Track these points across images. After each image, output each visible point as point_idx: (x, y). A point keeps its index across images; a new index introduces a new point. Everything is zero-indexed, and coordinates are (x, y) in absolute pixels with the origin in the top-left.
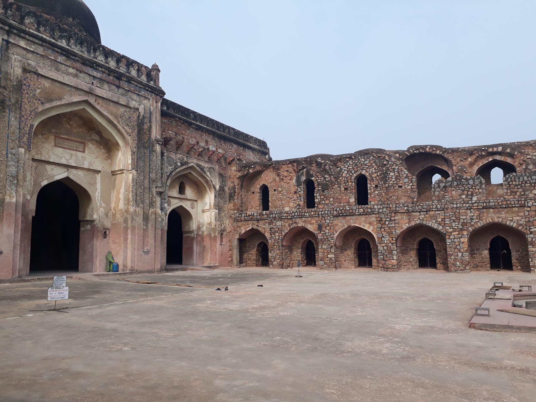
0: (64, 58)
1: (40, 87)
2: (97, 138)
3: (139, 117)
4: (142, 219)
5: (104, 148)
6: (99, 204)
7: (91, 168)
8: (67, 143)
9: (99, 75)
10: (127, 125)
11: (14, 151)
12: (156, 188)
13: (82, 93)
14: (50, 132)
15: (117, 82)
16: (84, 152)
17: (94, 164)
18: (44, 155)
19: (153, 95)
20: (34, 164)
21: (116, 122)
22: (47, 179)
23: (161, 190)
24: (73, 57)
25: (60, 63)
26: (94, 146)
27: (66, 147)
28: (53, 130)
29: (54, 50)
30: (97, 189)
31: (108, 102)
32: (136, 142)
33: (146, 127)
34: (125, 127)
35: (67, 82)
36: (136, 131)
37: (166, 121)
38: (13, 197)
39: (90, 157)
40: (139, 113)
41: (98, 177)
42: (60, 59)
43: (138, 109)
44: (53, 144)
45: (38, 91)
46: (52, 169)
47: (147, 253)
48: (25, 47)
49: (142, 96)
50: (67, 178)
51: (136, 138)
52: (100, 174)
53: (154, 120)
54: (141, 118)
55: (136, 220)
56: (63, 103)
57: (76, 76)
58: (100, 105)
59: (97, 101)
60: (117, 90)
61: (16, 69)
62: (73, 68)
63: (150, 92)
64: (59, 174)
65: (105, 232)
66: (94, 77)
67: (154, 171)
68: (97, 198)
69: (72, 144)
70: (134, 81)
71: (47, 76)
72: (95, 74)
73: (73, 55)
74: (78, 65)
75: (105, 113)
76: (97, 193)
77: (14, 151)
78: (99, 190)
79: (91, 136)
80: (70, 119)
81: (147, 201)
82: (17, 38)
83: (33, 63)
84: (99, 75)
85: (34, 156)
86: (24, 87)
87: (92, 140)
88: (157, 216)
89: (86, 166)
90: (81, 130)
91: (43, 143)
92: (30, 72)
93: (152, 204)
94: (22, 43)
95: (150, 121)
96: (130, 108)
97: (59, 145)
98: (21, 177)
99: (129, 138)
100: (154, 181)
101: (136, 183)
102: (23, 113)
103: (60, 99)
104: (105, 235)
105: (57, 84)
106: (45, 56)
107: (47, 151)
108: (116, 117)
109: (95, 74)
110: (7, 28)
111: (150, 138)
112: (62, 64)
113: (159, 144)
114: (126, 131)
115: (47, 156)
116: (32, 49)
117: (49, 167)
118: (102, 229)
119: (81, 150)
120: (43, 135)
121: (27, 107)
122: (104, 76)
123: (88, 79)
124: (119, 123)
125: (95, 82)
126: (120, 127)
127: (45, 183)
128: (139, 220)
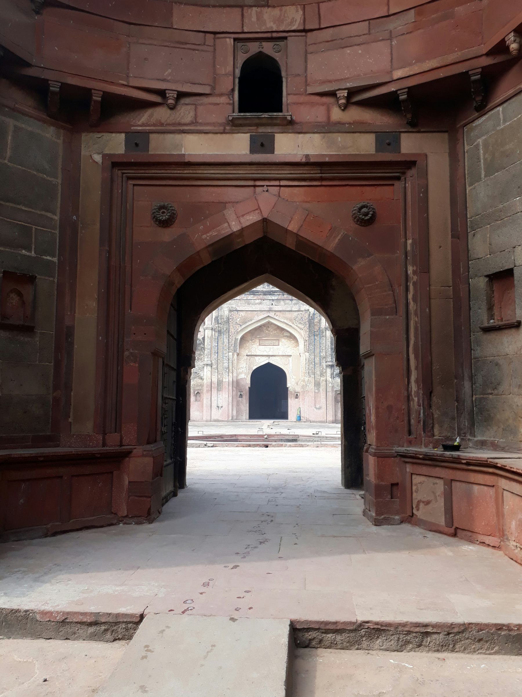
0: (252, 296)
2: (288, 334)
5: (293, 340)
8: (267, 342)
9: (276, 298)
10: (300, 323)
11: (226, 355)
13: (265, 312)
14: (256, 338)
20: (248, 358)
21: (291, 324)
23: (330, 364)
26: (286, 340)
31: (284, 312)
32: (307, 333)
33: (316, 320)
36: (308, 326)
41: (290, 359)
43: (308, 310)
44: (258, 344)
45: (238, 320)
47: (320, 408)
56: (253, 321)
57: (260, 303)
60: (291, 302)
61: (225, 312)
62: (258, 299)
64: (263, 361)
65: (297, 395)
66: (273, 300)
67: (324, 351)
72: (273, 298)
74: (261, 296)
75: (282, 320)
77: (226, 355)
81: (318, 373)
83: (234, 306)
86: (230, 320)
88: (328, 382)
92: (233, 311)
98: (231, 368)
102: (230, 334)
104: (297, 397)
108: (291, 320)
109: (273, 298)
111: (320, 328)
114: (299, 327)
118: (293, 393)
120: (252, 340)
121: (233, 330)
122: (280, 297)
123: (268, 302)
125: (273, 303)
128: (311, 386)
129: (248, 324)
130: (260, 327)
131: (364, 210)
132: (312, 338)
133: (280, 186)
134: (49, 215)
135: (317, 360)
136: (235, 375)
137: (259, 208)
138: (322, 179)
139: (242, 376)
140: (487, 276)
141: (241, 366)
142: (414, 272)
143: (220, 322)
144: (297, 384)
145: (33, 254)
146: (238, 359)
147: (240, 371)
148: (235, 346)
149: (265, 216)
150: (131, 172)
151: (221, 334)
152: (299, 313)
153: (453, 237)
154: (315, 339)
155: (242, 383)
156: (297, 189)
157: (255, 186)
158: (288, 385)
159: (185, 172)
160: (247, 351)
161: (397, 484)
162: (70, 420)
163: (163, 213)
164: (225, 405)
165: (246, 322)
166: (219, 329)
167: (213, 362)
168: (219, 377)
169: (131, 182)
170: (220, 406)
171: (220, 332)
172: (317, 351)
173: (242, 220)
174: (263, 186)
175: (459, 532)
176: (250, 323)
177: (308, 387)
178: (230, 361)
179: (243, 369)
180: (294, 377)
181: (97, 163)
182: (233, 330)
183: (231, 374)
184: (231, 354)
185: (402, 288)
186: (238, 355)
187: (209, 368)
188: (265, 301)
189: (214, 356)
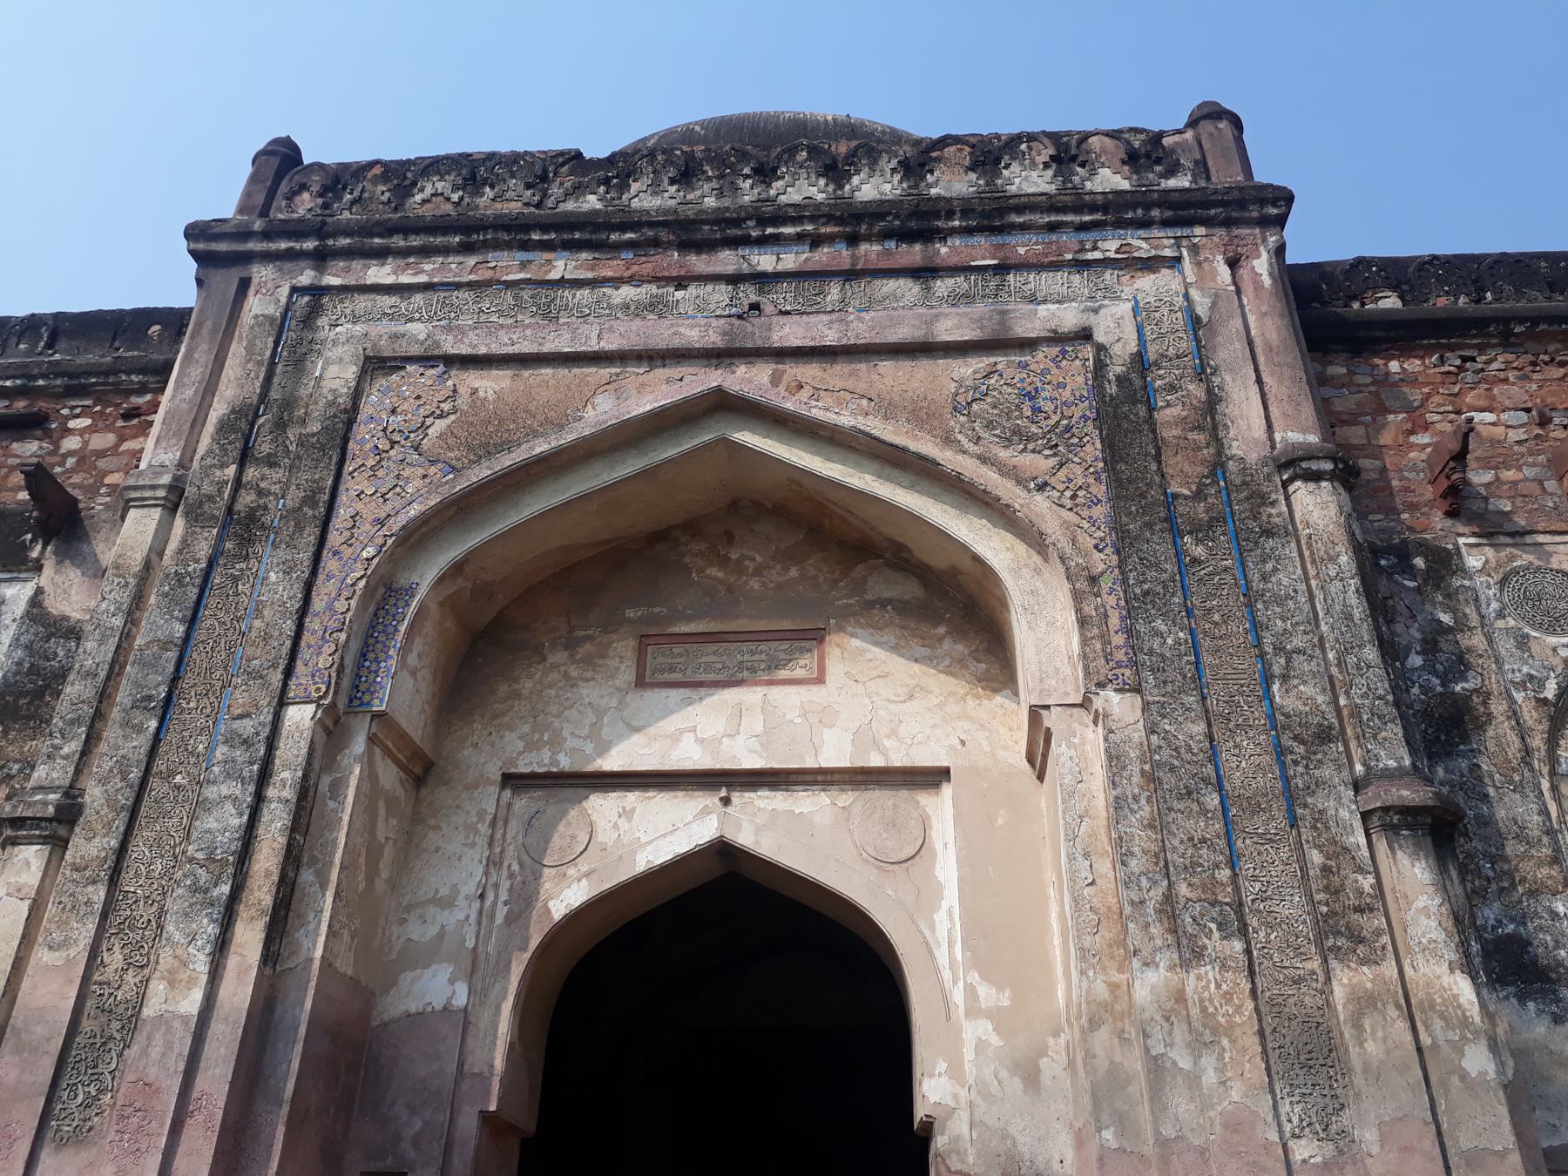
1: (446, 407)
2: (909, 589)
3: (1100, 367)
4: (1254, 1070)
5: (957, 632)
6: (958, 996)
7: (876, 761)
8: (710, 655)
9: (790, 260)
10: (1016, 437)
12: (1357, 786)
14: (612, 624)
15: (913, 253)
16: (820, 680)
17: (893, 733)
18: (570, 743)
19: (1199, 231)
20: (522, 804)
21: (925, 446)
22: (587, 875)
24: (629, 236)
25: (562, 282)
26: (890, 637)
27: (712, 677)
28: (630, 613)
29: (525, 246)
30: (938, 892)
32: (1100, 512)
33: (1170, 413)
34: (1003, 454)
35: (593, 345)
36: (1093, 449)
37: (1414, 365)
38: (191, 982)
39: (864, 695)
40: (1101, 348)
41: (940, 807)
42: (561, 266)
43: (1085, 335)
44: (627, 674)
45: (439, 426)
46: (627, 814)
48: (390, 280)
49: (1106, 263)
50: (722, 850)
51: (1100, 490)
52: (947, 790)
53: (1228, 350)
54: (1116, 369)
55: (1193, 1080)
57: (655, 306)
58: (805, 394)
59: (786, 378)
63: (1166, 223)
66: (762, 280)
68: (942, 956)
69: (742, 653)
70: (1020, 210)
71: (483, 350)
72: (765, 261)
73: (623, 227)
75: (845, 420)
76: (941, 918)
78: (951, 898)
79: (859, 587)
80: (730, 538)
81: (1292, 907)
82: (356, 264)
84: (790, 260)
85: (512, 762)
87: (870, 605)
89: (835, 753)
90: (794, 573)
91: (572, 683)
93: (1345, 925)
94: (380, 274)
95: (1203, 373)
96: (1029, 344)
97: (667, 677)
99: (1039, 508)
100: (1324, 736)
101: (1151, 778)
105: (547, 372)
106: (488, 284)
107: (590, 718)
108: (921, 415)
109: (765, 261)
110: (310, 245)
111: (1219, 463)
112: (578, 284)
113: (1315, 477)
114: (1005, 470)
115: (589, 748)
116: (423, 279)
117: (602, 806)
119: (799, 673)
120: (571, 645)
123: (720, 295)
124: (948, 440)
126: (967, 466)
132: (1160, 547)
135: (1247, 764)
141: (436, 881)
143: (264, 447)
144: (1031, 1078)
147: (419, 931)
151: (246, 541)
152: (1001, 361)
154: (1186, 564)
158: (934, 1089)
160: (512, 742)
165: (507, 446)
166: (247, 499)
167: (94, 794)
168: (114, 959)
172: (1231, 664)
177: (1181, 1104)
179: (451, 918)
180: (983, 990)
183: (249, 938)
184: (300, 716)
188: (693, 290)
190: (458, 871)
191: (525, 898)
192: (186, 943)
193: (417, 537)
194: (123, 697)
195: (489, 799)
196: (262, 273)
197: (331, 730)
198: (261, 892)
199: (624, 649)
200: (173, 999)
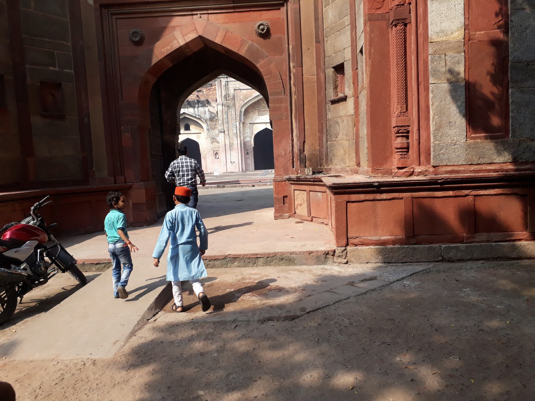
8: (264, 112)
14: (256, 110)
83: (237, 86)
98: (238, 133)
103: (251, 96)
121: (238, 105)
127: (256, 132)
129: (248, 100)
130: (258, 101)
131: (261, 27)
133: (208, 14)
134: (64, 43)
136: (242, 138)
137: (196, 29)
138: (234, 8)
139: (248, 139)
140: (333, 68)
141: (246, 132)
142: (294, 67)
145: (57, 69)
146: (243, 127)
148: (240, 117)
149: (200, 34)
150: (113, 10)
153: (316, 42)
155: (248, 144)
156: (219, 15)
157: (192, 15)
159: (147, 8)
161: (287, 196)
162: (94, 169)
163: (136, 36)
164: (237, 161)
165: (247, 98)
169: (114, 17)
170: (233, 161)
171: (228, 107)
173: (186, 38)
174: (197, 14)
175: (314, 219)
176: (250, 98)
178: (238, 128)
181: (90, 5)
182: (238, 105)
183: (239, 138)
184: (238, 123)
185: (288, 77)
186: (243, 123)
187: (223, 134)
189: (226, 126)
190: (248, 131)
191: (252, 133)
192: (235, 138)
193: (242, 107)
194: (225, 122)
195: (249, 125)
196: (222, 79)
197: (240, 123)
198: (239, 136)
199: (257, 112)
200: (235, 142)
